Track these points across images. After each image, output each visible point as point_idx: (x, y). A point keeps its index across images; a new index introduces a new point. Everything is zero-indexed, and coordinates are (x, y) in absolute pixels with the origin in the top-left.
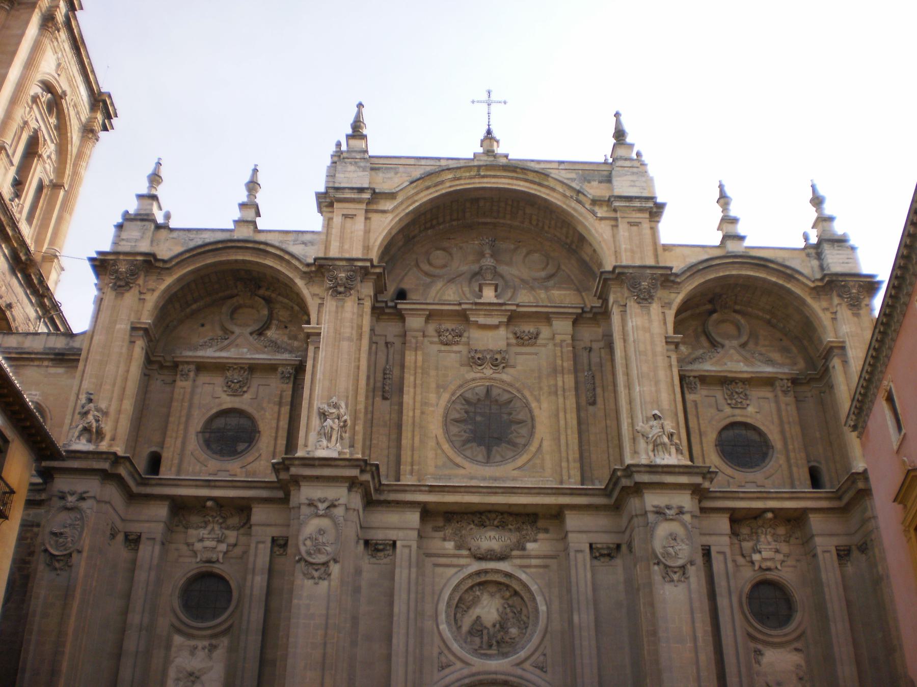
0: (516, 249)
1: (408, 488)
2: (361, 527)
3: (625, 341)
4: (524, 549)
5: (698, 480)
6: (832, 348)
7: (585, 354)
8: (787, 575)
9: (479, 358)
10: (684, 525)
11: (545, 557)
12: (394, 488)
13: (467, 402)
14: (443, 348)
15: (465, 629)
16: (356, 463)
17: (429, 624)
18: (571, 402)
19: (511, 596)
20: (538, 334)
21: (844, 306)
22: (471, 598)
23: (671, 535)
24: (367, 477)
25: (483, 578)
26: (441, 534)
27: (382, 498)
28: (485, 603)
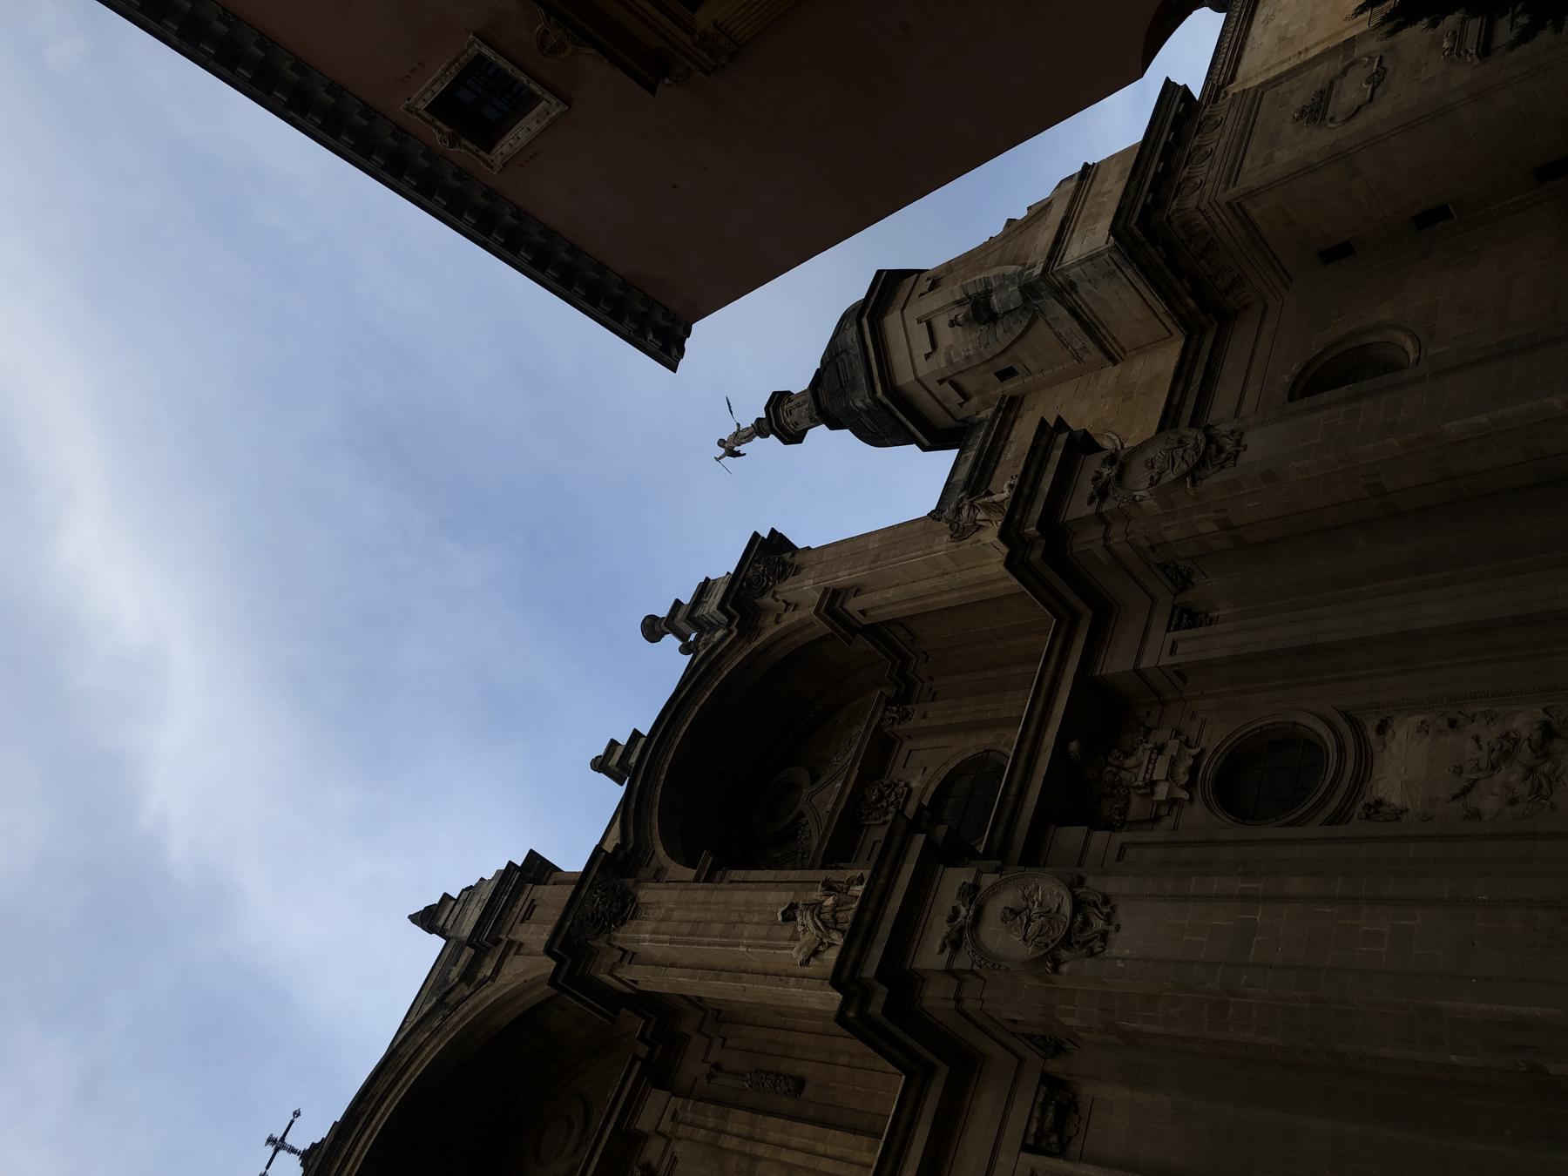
3: (673, 965)
5: (920, 839)
6: (830, 610)
8: (1215, 736)
10: (995, 889)
18: (773, 1128)
21: (779, 588)
23: (1004, 919)
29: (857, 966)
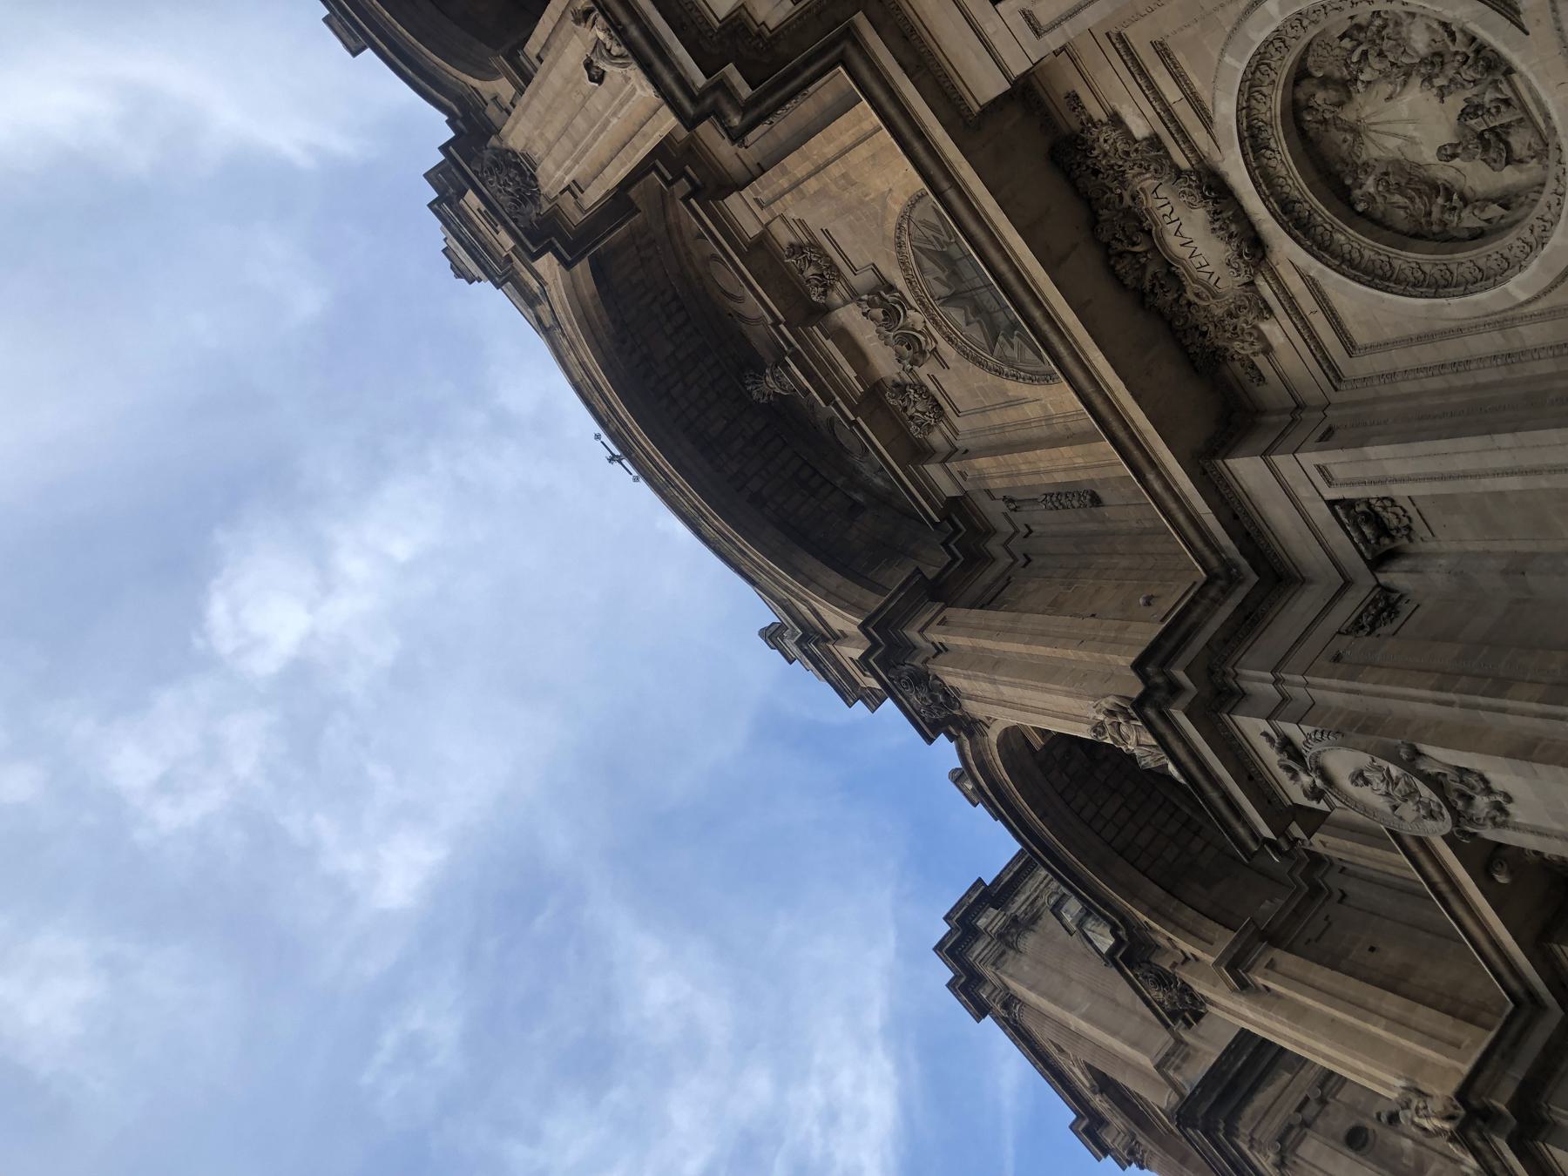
0: (739, 315)
1: (1181, 518)
2: (1347, 584)
4: (1154, 141)
7: (750, 137)
9: (909, 348)
11: (1139, 71)
12: (1199, 544)
13: (993, 334)
14: (948, 409)
15: (1510, 177)
16: (1161, 727)
17: (1531, 335)
19: (1325, 82)
20: (796, 249)
22: (1397, 198)
24: (1180, 675)
25: (1312, 202)
26: (1260, 361)
27: (1243, 562)
28: (1392, 143)
29: (683, 82)
